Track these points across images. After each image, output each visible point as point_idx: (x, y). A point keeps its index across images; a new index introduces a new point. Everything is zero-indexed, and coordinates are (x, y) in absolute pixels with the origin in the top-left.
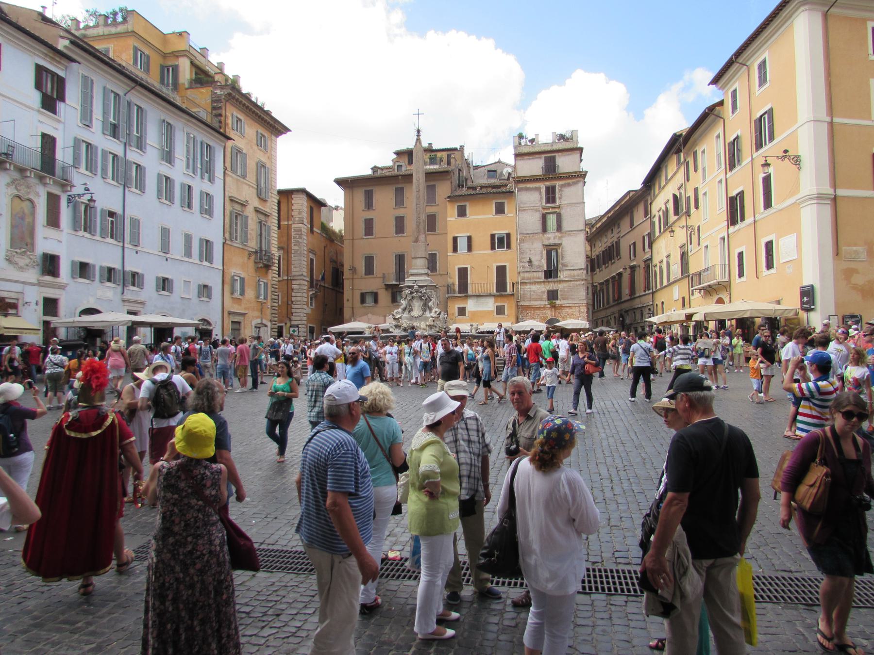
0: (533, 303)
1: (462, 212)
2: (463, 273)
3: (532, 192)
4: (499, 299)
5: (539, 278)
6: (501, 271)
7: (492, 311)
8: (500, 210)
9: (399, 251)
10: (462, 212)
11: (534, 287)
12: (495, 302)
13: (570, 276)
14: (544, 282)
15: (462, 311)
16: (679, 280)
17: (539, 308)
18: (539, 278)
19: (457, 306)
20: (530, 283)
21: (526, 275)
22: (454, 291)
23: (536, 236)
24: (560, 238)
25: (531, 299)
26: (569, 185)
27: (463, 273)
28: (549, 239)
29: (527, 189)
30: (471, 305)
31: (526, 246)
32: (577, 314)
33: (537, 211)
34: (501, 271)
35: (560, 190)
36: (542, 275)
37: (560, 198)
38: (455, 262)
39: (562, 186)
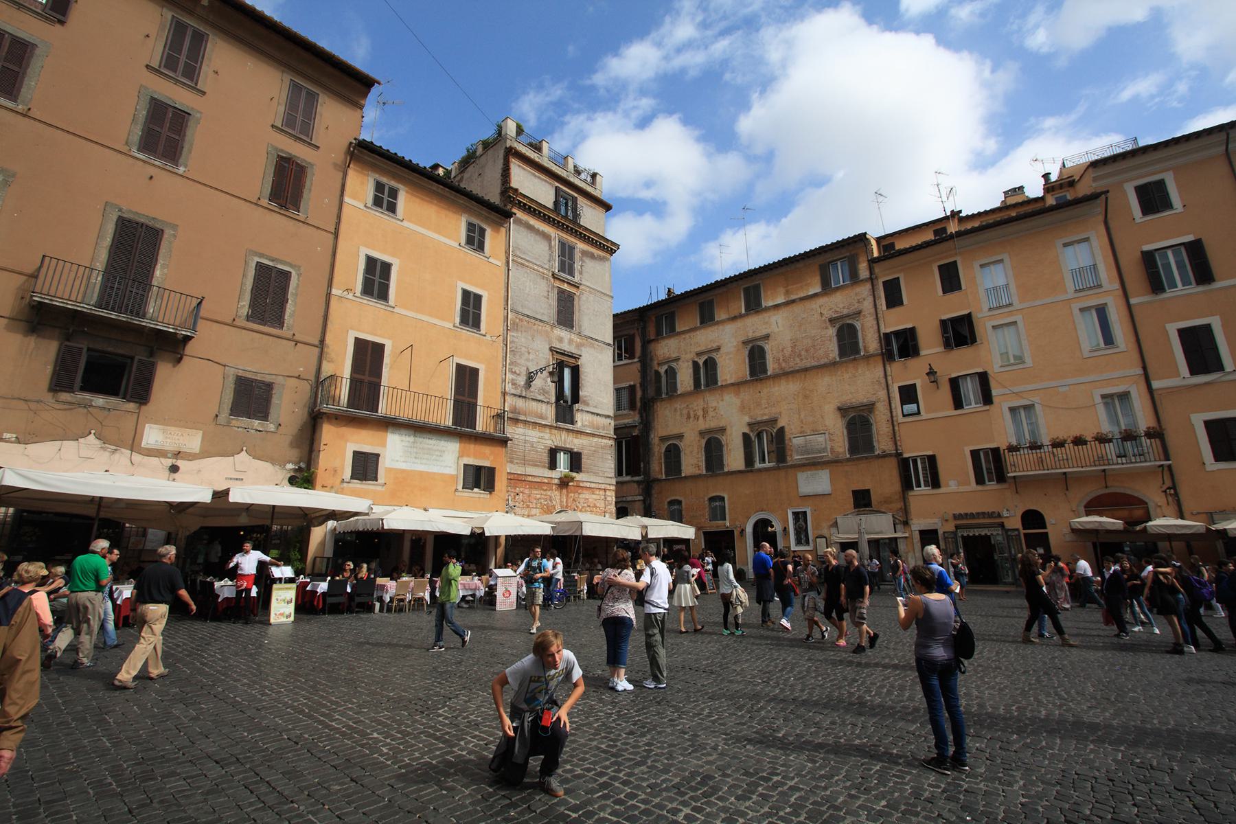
0: (531, 470)
1: (385, 201)
2: (369, 357)
3: (538, 238)
4: (472, 447)
5: (541, 417)
6: (466, 379)
7: (454, 478)
8: (475, 241)
9: (144, 208)
10: (385, 201)
11: (533, 435)
12: (461, 456)
13: (592, 426)
14: (551, 427)
15: (365, 467)
16: (836, 462)
17: (539, 485)
18: (541, 417)
19: (351, 448)
20: (526, 422)
21: (520, 403)
22: (335, 400)
23: (540, 326)
24: (579, 346)
25: (525, 462)
26: (592, 256)
27: (369, 357)
28: (561, 340)
29: (531, 228)
30: (395, 451)
31: (519, 338)
32: (602, 505)
33: (543, 277)
34: (466, 379)
35: (581, 260)
36: (549, 412)
37: (581, 273)
38: (355, 319)
39: (584, 253)
